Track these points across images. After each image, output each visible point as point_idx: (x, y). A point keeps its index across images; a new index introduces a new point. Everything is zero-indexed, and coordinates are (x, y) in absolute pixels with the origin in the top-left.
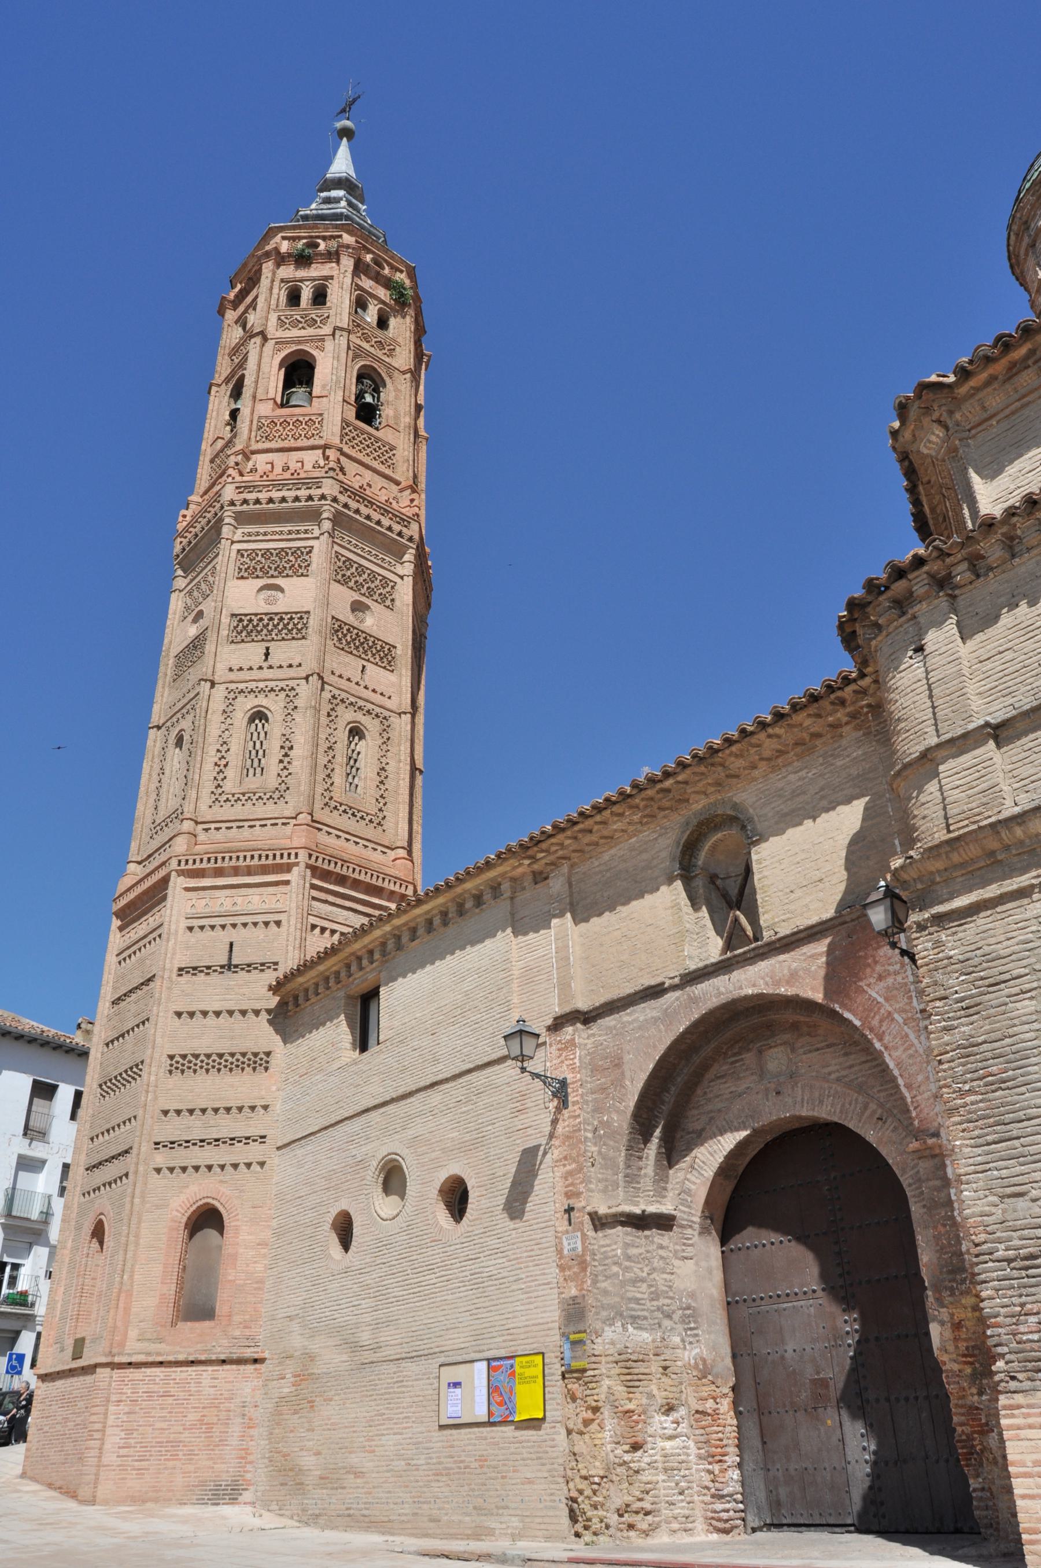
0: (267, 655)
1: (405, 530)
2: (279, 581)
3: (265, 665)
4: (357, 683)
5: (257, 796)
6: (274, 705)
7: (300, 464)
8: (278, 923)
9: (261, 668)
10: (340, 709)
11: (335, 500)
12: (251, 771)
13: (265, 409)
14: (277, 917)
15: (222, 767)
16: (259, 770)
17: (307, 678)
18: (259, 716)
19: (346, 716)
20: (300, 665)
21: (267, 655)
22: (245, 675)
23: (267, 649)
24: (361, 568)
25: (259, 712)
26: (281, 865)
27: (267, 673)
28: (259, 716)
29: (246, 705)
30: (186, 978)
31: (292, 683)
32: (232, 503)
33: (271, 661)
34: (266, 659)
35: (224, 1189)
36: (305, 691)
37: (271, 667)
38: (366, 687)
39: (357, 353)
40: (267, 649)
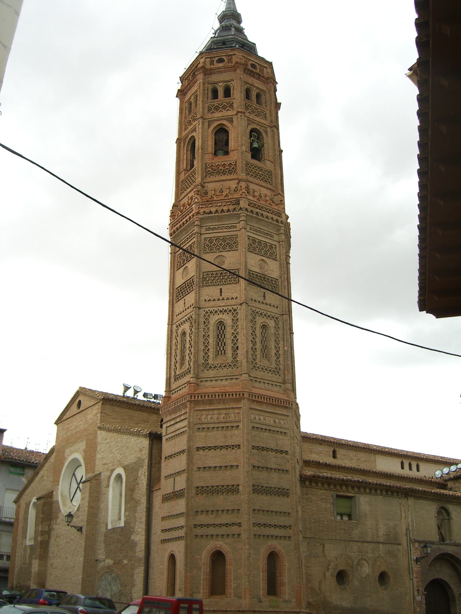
0: (221, 292)
1: (279, 219)
2: (223, 254)
3: (221, 298)
4: (263, 303)
5: (224, 364)
6: (227, 319)
7: (228, 190)
8: (238, 426)
9: (219, 300)
10: (258, 318)
11: (246, 209)
12: (220, 352)
13: (209, 158)
14: (236, 424)
15: (206, 351)
16: (223, 351)
17: (241, 304)
18: (221, 324)
19: (260, 321)
20: (236, 298)
21: (221, 292)
22: (212, 303)
23: (221, 289)
24: (260, 242)
25: (221, 321)
26: (236, 399)
27: (221, 303)
28: (221, 324)
29: (214, 319)
30: (201, 452)
31: (235, 307)
32: (198, 213)
33: (224, 295)
34: (221, 295)
35: (226, 546)
36: (242, 312)
37: (223, 299)
38: (266, 304)
39: (250, 121)
40: (221, 289)
